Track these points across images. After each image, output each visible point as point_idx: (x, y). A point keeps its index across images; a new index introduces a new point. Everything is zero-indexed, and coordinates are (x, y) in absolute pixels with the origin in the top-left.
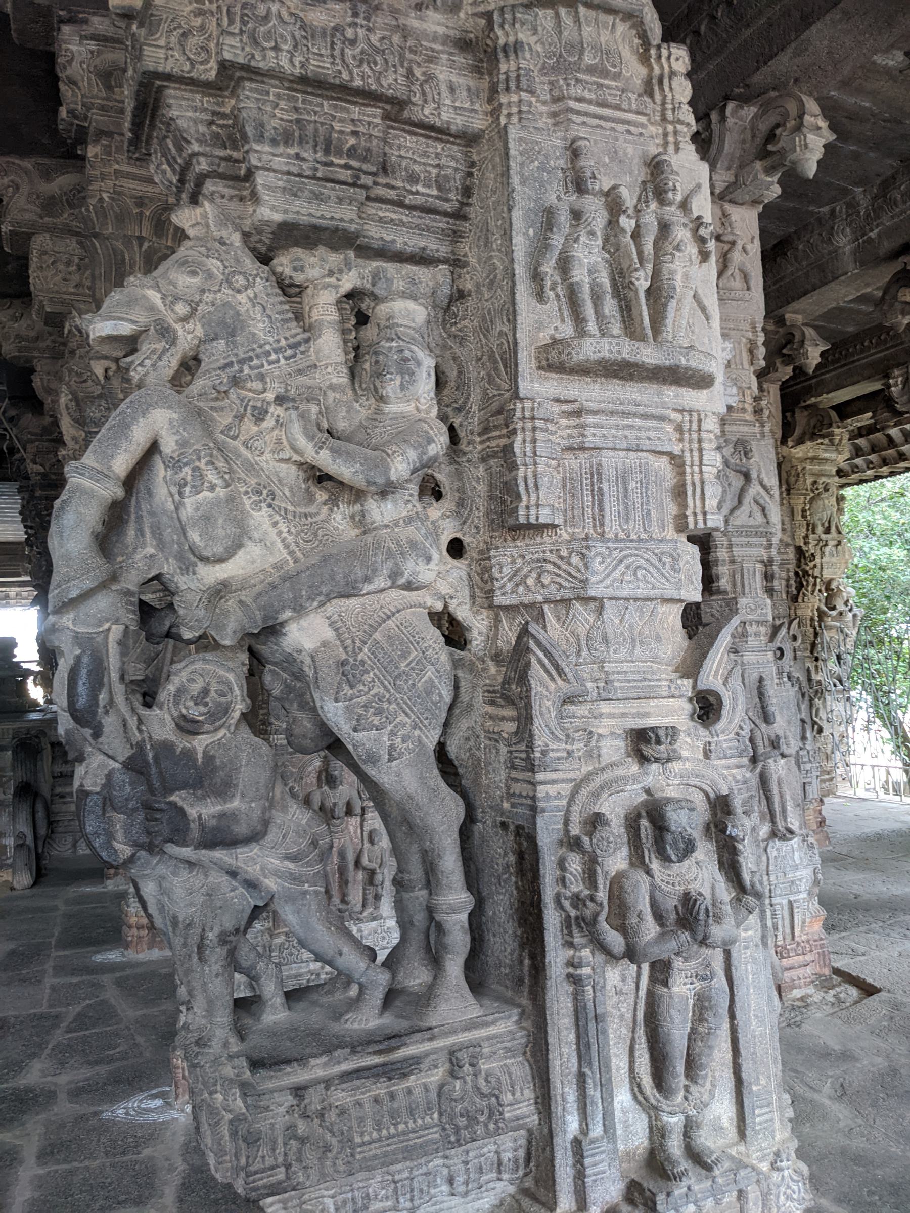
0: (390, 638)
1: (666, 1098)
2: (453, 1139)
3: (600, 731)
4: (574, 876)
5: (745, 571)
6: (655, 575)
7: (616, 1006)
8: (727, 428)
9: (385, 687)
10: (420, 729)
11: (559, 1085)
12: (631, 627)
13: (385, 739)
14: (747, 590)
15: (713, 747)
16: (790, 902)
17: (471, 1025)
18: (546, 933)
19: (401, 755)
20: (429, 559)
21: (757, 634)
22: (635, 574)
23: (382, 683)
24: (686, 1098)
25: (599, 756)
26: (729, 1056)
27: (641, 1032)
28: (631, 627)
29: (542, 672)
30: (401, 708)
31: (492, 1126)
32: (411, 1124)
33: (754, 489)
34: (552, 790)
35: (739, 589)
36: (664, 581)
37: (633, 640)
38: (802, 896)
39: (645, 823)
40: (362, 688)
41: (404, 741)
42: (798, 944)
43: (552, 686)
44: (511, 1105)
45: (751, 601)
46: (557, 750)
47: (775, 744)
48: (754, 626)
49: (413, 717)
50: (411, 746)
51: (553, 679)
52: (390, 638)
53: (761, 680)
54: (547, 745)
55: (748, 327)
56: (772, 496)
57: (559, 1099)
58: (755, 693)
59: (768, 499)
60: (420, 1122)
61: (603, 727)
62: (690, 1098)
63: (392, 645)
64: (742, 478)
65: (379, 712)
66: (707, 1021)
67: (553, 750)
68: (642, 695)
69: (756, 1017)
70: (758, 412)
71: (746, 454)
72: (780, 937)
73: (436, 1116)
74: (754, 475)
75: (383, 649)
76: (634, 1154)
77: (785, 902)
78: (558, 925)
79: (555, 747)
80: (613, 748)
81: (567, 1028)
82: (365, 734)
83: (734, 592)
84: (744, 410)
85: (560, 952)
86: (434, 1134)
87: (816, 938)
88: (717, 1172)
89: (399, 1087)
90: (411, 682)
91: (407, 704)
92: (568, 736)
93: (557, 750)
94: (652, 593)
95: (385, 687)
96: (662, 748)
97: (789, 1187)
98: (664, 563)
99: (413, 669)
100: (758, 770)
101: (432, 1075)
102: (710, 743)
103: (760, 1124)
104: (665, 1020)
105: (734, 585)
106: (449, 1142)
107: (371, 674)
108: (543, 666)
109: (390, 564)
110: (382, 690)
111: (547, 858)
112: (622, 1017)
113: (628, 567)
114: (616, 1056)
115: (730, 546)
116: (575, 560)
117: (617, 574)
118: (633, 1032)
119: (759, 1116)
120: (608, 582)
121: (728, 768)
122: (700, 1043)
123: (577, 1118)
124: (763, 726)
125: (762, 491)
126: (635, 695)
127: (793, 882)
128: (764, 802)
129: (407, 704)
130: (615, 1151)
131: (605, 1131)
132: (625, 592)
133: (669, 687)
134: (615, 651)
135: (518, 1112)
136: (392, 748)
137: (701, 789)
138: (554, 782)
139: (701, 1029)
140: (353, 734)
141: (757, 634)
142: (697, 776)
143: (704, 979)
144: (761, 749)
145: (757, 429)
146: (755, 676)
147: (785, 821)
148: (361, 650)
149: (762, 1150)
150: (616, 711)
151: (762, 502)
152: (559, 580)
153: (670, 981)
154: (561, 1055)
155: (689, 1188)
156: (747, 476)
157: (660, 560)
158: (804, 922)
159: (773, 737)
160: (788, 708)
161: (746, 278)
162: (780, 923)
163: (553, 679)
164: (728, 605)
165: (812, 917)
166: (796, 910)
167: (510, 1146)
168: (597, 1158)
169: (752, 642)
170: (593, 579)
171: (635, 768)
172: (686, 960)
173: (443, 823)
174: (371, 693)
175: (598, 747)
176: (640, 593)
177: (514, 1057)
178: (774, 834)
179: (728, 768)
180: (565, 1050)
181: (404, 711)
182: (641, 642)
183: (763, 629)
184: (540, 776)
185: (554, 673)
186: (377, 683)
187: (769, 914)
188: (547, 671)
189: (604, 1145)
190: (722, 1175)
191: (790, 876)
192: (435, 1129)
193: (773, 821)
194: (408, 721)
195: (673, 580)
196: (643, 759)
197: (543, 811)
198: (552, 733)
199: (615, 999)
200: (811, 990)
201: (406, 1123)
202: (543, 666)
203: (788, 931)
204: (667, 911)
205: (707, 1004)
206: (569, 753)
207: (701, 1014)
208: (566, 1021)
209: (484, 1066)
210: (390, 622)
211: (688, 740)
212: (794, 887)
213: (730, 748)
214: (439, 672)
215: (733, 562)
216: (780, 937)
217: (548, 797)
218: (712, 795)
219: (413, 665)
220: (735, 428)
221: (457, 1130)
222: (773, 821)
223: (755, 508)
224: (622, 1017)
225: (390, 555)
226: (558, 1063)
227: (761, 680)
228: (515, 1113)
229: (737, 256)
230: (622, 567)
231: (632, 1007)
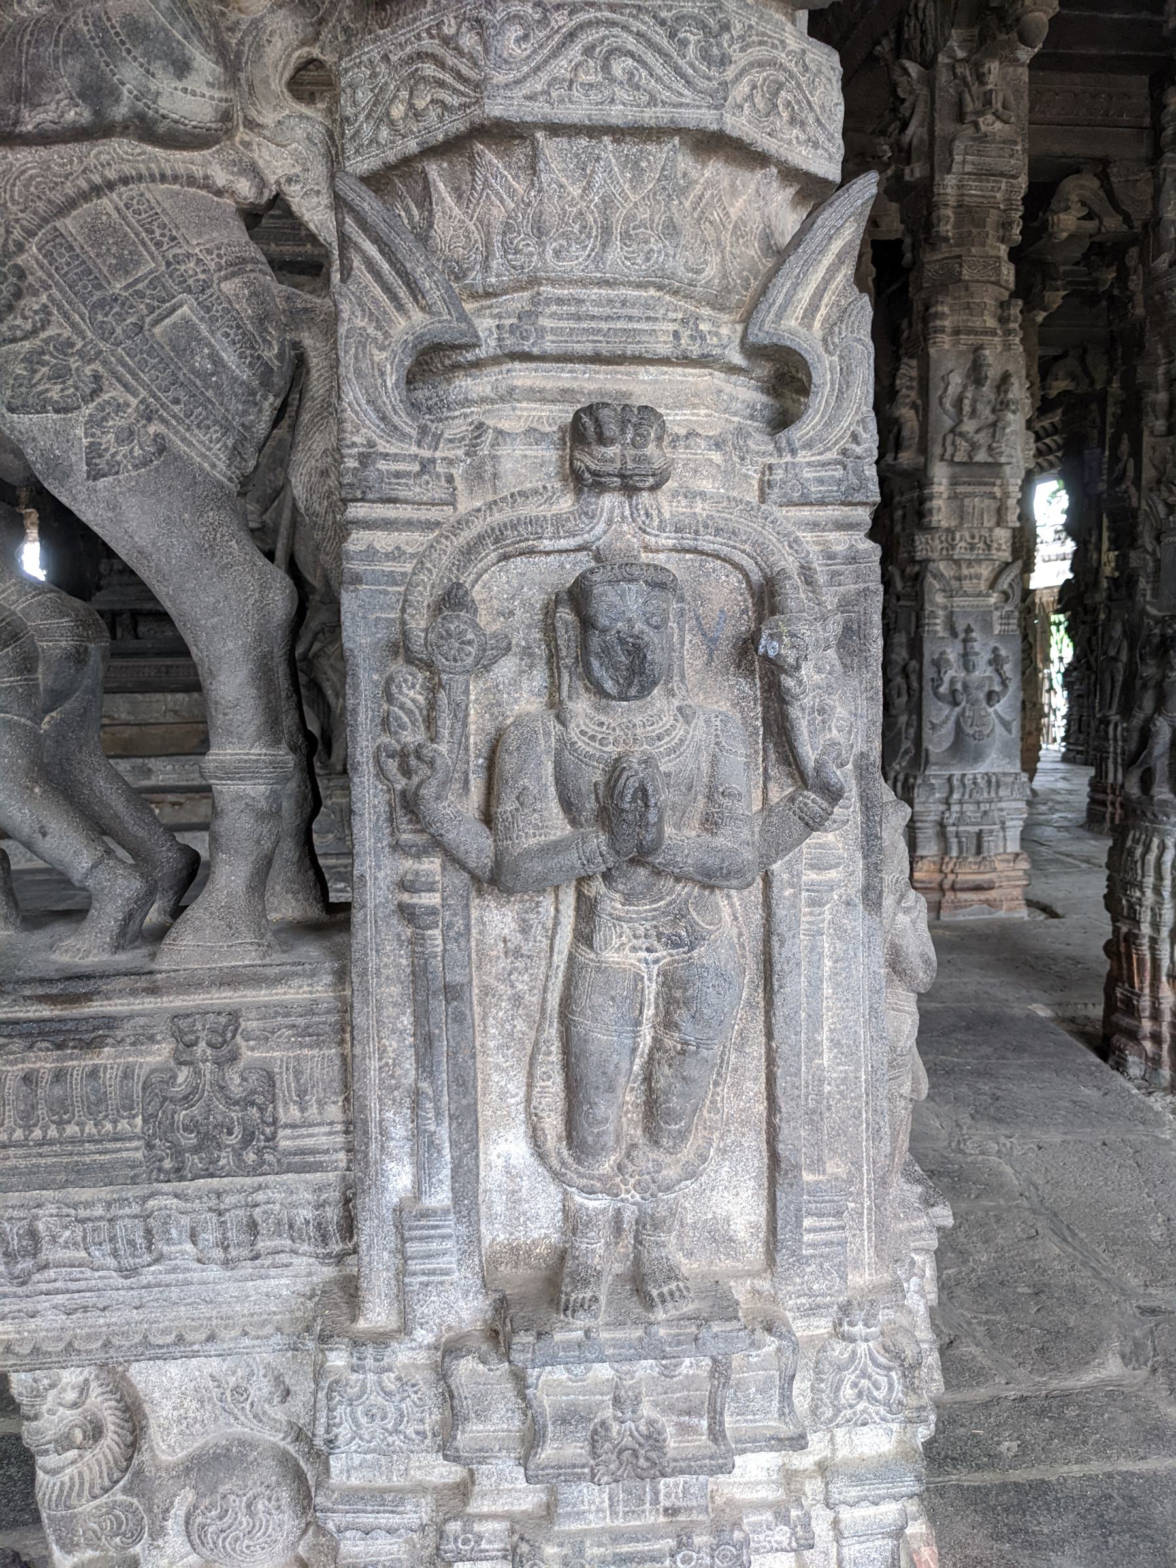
0: (95, 232)
1: (579, 1161)
2: (167, 1164)
3: (505, 425)
4: (409, 713)
6: (659, 70)
7: (506, 978)
9: (74, 325)
10: (163, 421)
11: (374, 1104)
12: (607, 203)
13: (80, 432)
15: (779, 475)
17: (231, 979)
18: (356, 823)
19: (114, 469)
20: (182, 68)
22: (606, 68)
23: (67, 316)
24: (620, 1168)
25: (495, 476)
26: (761, 1108)
27: (552, 1031)
28: (607, 203)
29: (377, 290)
30: (114, 373)
31: (250, 1157)
32: (90, 1128)
34: (382, 540)
36: (679, 86)
37: (606, 230)
39: (565, 614)
40: (19, 322)
41: (120, 441)
43: (403, 323)
44: (293, 1126)
46: (396, 458)
49: (143, 393)
50: (137, 452)
51: (400, 307)
52: (95, 232)
54: (371, 444)
57: (374, 1130)
60: (109, 1126)
61: (513, 419)
62: (631, 1168)
63: (97, 244)
65: (60, 375)
66: (677, 1025)
67: (385, 456)
68: (605, 349)
69: (836, 1044)
73: (139, 1121)
75: (71, 248)
76: (528, 1253)
78: (383, 808)
79: (392, 450)
80: (528, 464)
81: (395, 1005)
82: (35, 417)
85: (386, 861)
86: (136, 1152)
88: (660, 1315)
89: (79, 1063)
90: (132, 320)
91: (124, 365)
92: (424, 430)
93: (396, 458)
94: (650, 116)
95: (74, 325)
96: (612, 451)
97: (864, 1374)
98: (684, 43)
99: (140, 295)
101: (150, 1053)
102: (770, 467)
103: (813, 1245)
104: (582, 1013)
106: (160, 1170)
107: (44, 298)
108: (378, 276)
109: (75, 64)
110: (67, 332)
111: (362, 675)
112: (517, 1000)
113: (588, 51)
114: (498, 1068)
116: (468, 41)
117: (561, 67)
118: (539, 1031)
119: (809, 1231)
120: (537, 85)
121: (814, 526)
122: (666, 1070)
123: (408, 1168)
126: (588, 348)
129: (124, 365)
130: (475, 1239)
131: (456, 1199)
132: (578, 111)
133: (676, 334)
134: (557, 253)
135: (309, 1142)
136: (94, 451)
137: (737, 566)
138: (387, 525)
139: (668, 1043)
140: (8, 415)
142: (718, 531)
143: (676, 945)
148: (20, 248)
149: (811, 1294)
150: (550, 385)
152: (443, 95)
153: (598, 939)
154: (382, 1051)
155: (587, 1332)
157: (672, 36)
163: (400, 307)
167: (297, 1196)
168: (434, 1246)
170: (499, 78)
171: (566, 503)
172: (628, 899)
173: (216, 611)
174: (43, 335)
175: (493, 457)
176: (617, 114)
177: (318, 1045)
179: (814, 526)
180: (392, 1044)
181: (119, 380)
182: (626, 236)
184: (357, 511)
185: (402, 292)
186: (56, 315)
188: (388, 289)
189: (450, 1225)
190: (669, 1322)
192: (135, 1144)
194: (134, 402)
195: (703, 84)
196: (583, 482)
197: (357, 579)
198: (384, 418)
199: (504, 963)
201: (81, 1124)
202: (378, 276)
204: (579, 794)
205: (678, 994)
206: (426, 466)
207: (667, 1013)
208: (395, 990)
209: (249, 1054)
210: (105, 200)
211: (716, 457)
213: (821, 481)
214: (208, 310)
217: (370, 554)
218: (756, 576)
219: (140, 286)
221: (177, 1152)
224: (517, 1000)
225: (75, 44)
226: (374, 1064)
228: (298, 1142)
230: (575, 51)
231: (539, 984)
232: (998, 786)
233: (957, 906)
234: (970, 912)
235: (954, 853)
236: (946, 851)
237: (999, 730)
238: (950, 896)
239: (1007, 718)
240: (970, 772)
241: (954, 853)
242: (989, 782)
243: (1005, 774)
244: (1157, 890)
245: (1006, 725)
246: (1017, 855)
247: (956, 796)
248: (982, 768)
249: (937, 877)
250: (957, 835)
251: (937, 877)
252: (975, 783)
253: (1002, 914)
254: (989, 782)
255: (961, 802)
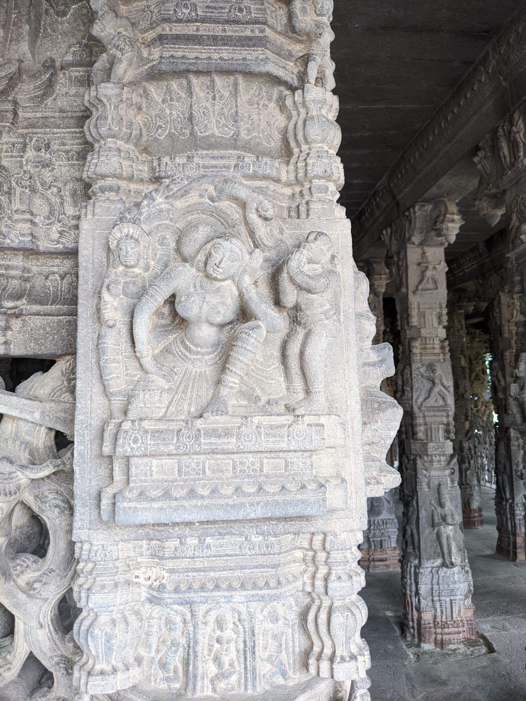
5: (433, 429)
8: (423, 358)
14: (434, 439)
16: (451, 600)
21: (439, 461)
33: (438, 388)
35: (429, 438)
38: (458, 597)
42: (455, 622)
45: (434, 444)
47: (444, 518)
48: (438, 457)
53: (439, 485)
55: (437, 306)
56: (449, 391)
58: (436, 491)
59: (446, 392)
64: (431, 383)
70: (442, 348)
71: (432, 371)
72: (444, 617)
74: (437, 381)
77: (448, 600)
83: (427, 440)
84: (434, 348)
87: (468, 619)
100: (436, 531)
105: (427, 436)
115: (424, 417)
124: (439, 509)
125: (443, 389)
127: (452, 590)
128: (439, 548)
141: (439, 461)
144: (436, 521)
145: (441, 357)
146: (437, 482)
147: (451, 558)
151: (442, 394)
156: (434, 383)
158: (460, 611)
159: (443, 515)
160: (456, 500)
161: (435, 282)
162: (444, 610)
164: (423, 446)
165: (466, 609)
166: (454, 605)
169: (436, 465)
178: (444, 565)
183: (443, 458)
187: (438, 605)
191: (452, 586)
193: (443, 557)
200: (461, 646)
203: (449, 614)
212: (453, 593)
215: (425, 424)
216: (444, 617)
220: (428, 358)
222: (443, 557)
223: (439, 397)
227: (439, 485)
229: (429, 273)
232: (386, 524)
233: (375, 567)
234: (380, 569)
235: (373, 548)
236: (370, 547)
237: (386, 503)
238: (372, 563)
239: (389, 499)
240: (377, 519)
241: (373, 548)
242: (383, 523)
243: (389, 519)
244: (410, 579)
245: (388, 502)
246: (395, 548)
247: (372, 527)
248: (381, 517)
249: (368, 556)
250: (373, 541)
251: (368, 556)
252: (378, 523)
253: (391, 570)
254: (383, 523)
255: (374, 530)
